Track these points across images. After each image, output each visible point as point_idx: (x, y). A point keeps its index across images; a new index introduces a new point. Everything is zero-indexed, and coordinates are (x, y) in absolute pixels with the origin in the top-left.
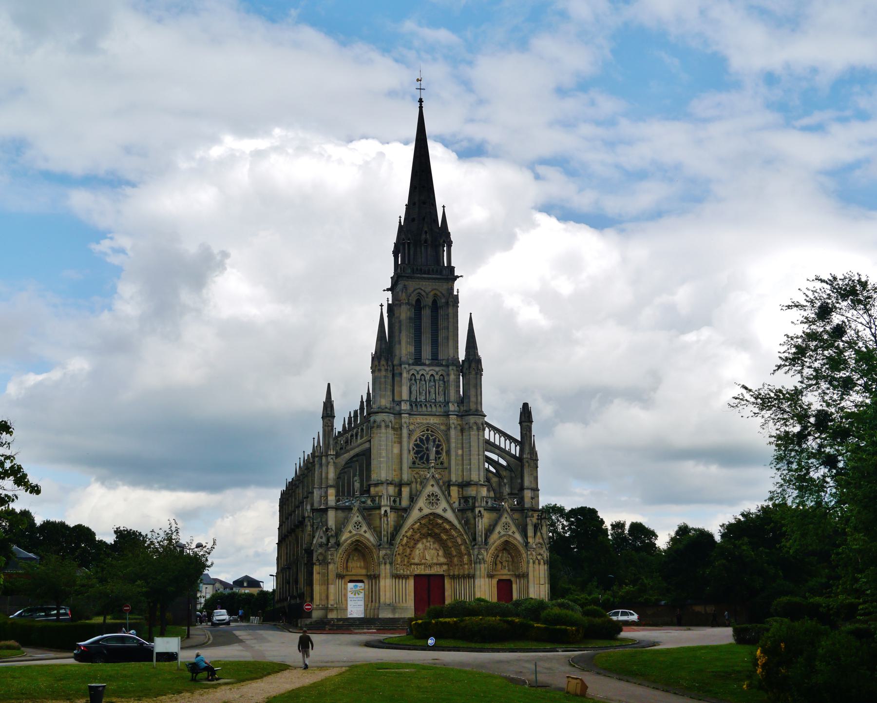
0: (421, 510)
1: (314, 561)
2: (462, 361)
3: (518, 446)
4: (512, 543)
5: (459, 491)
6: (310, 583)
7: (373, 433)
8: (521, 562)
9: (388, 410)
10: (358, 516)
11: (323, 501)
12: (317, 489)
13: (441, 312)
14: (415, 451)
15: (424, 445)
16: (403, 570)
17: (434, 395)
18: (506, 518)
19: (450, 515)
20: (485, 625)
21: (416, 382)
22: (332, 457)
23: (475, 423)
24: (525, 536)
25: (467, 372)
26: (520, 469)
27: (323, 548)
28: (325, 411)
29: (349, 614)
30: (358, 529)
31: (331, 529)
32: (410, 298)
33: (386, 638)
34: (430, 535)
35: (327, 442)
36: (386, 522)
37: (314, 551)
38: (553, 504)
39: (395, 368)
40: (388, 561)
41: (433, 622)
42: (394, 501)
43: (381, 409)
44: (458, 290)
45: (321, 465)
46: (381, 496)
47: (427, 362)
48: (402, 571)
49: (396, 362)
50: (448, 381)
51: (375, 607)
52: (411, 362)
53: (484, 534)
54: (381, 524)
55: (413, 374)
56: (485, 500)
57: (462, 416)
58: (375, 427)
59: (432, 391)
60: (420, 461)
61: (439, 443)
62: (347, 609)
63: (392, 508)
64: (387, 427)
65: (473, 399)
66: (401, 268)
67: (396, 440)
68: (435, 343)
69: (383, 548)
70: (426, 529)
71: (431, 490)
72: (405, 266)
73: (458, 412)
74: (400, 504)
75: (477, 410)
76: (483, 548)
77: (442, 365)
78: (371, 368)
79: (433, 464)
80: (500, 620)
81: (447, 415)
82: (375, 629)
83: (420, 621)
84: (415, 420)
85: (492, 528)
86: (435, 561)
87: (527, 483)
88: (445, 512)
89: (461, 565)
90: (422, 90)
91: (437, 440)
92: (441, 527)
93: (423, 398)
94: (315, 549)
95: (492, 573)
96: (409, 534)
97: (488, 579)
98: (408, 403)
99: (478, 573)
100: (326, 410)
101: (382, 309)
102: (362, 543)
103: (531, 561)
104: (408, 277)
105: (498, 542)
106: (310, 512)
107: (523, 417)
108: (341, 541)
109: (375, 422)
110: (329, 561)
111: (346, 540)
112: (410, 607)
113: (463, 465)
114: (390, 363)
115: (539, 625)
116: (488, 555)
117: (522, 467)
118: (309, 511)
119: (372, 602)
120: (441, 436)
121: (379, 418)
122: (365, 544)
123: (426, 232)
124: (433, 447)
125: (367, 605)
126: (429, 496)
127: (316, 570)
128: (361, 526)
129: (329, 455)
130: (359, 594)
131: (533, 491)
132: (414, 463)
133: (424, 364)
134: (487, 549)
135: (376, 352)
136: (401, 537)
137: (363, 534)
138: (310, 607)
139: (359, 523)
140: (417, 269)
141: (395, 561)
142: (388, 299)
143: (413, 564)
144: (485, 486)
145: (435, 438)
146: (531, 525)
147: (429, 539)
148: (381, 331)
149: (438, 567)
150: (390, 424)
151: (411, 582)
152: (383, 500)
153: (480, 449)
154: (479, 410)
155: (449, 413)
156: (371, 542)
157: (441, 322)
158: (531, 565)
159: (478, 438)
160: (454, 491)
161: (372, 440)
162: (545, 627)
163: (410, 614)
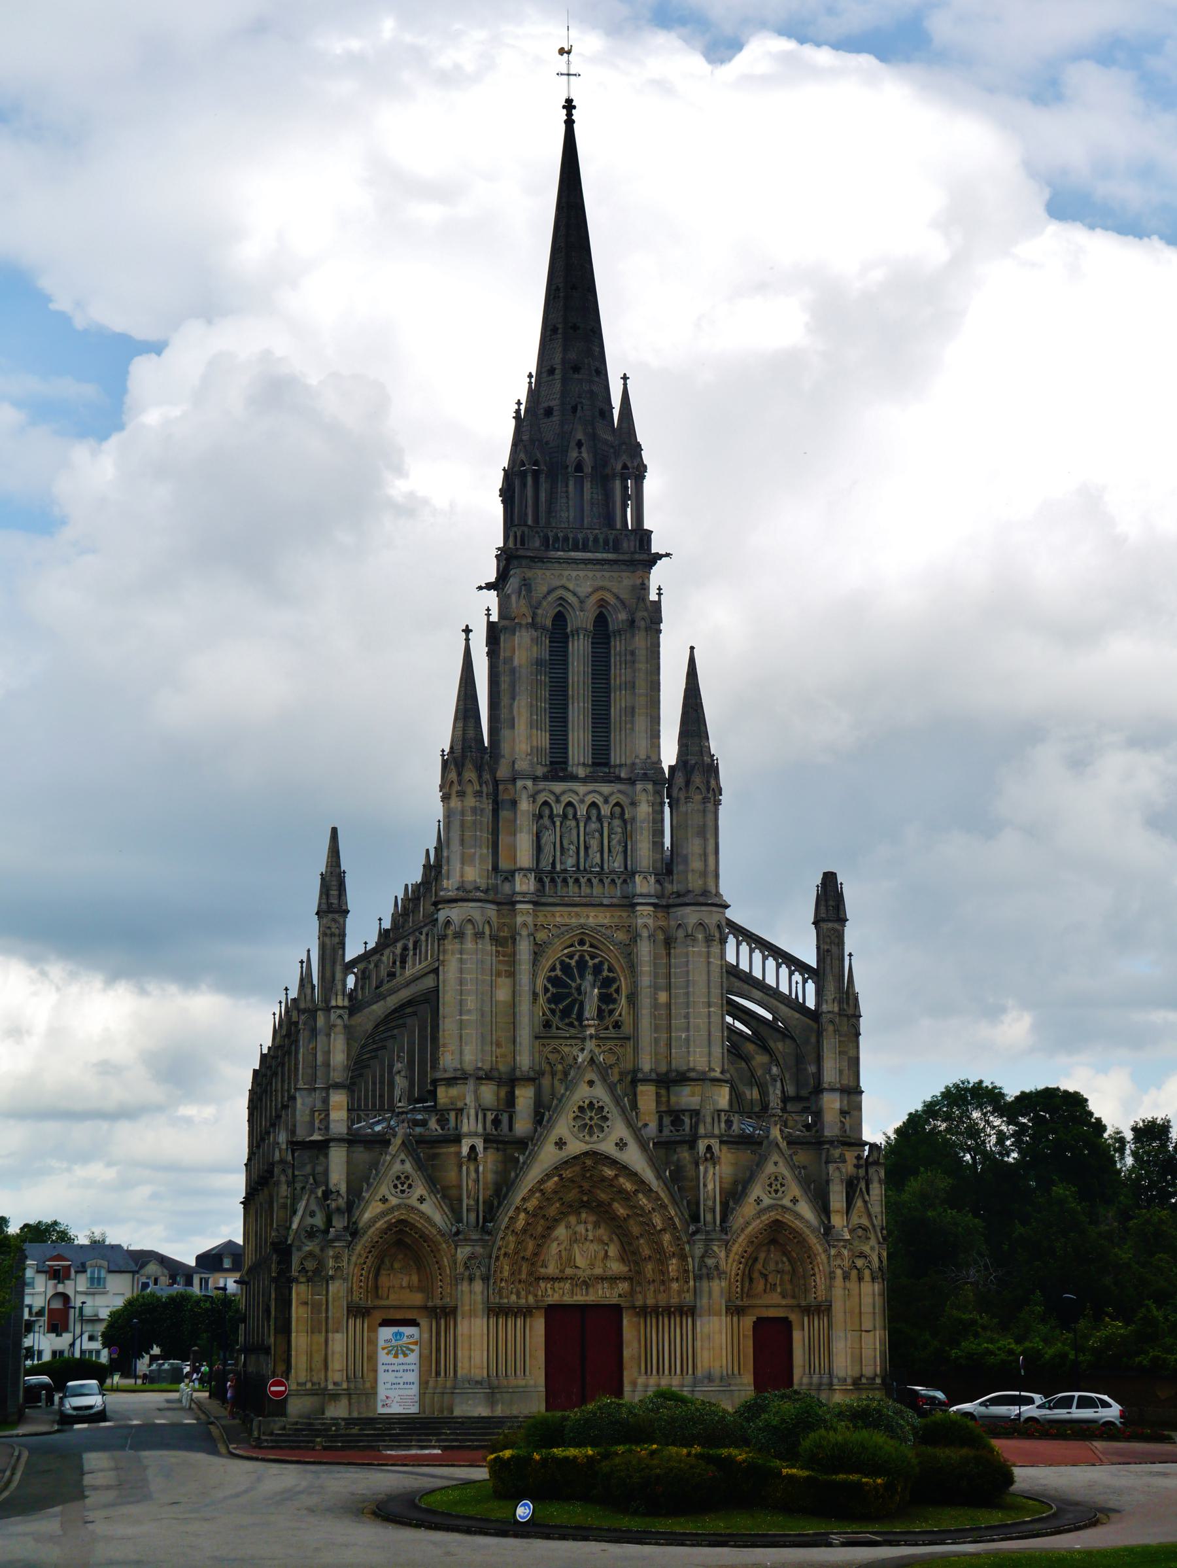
0: (560, 1144)
1: (294, 1274)
2: (671, 767)
3: (810, 981)
4: (790, 1227)
5: (657, 1093)
6: (285, 1329)
7: (444, 951)
8: (814, 1275)
9: (482, 894)
10: (403, 1162)
11: (317, 1122)
12: (305, 1093)
13: (617, 645)
14: (549, 995)
15: (574, 980)
16: (518, 1297)
17: (598, 855)
18: (776, 1163)
19: (634, 1157)
20: (658, 1471)
21: (554, 823)
22: (339, 1012)
23: (700, 923)
24: (824, 1209)
25: (682, 796)
26: (813, 1040)
27: (317, 1241)
28: (324, 897)
29: (380, 1404)
30: (403, 1192)
31: (338, 1191)
32: (540, 611)
33: (440, 1483)
34: (585, 1205)
35: (328, 974)
36: (473, 1175)
37: (294, 1249)
38: (973, 1080)
39: (501, 787)
40: (478, 1274)
41: (537, 1457)
42: (496, 1122)
43: (465, 890)
44: (659, 589)
45: (314, 1032)
46: (461, 1110)
47: (581, 772)
48: (514, 1297)
49: (503, 772)
50: (633, 819)
51: (445, 1388)
52: (540, 771)
53: (721, 1202)
54: (461, 1180)
55: (546, 803)
56: (723, 1118)
57: (668, 906)
58: (450, 937)
59: (594, 844)
60: (562, 1019)
61: (611, 975)
62: (375, 1394)
63: (487, 1140)
64: (479, 935)
65: (696, 864)
66: (516, 537)
67: (503, 968)
68: (601, 722)
69: (466, 1240)
70: (577, 1190)
71: (586, 1095)
72: (526, 529)
73: (657, 897)
74: (511, 1128)
75: (705, 893)
76: (719, 1240)
77: (619, 779)
78: (442, 787)
79: (592, 1031)
80: (699, 1456)
81: (629, 904)
82: (439, 1447)
83: (507, 1453)
84: (550, 919)
85: (740, 1188)
86: (598, 1271)
87: (830, 1075)
88: (621, 1149)
89: (663, 1282)
90: (572, 78)
91: (606, 967)
92: (611, 1186)
93: (570, 861)
94: (297, 1243)
95: (739, 1303)
96: (531, 1205)
97: (729, 1319)
99: (704, 1301)
100: (328, 896)
101: (467, 640)
102: (413, 1226)
103: (839, 1272)
104: (532, 559)
105: (755, 1225)
106: (287, 1149)
107: (823, 909)
108: (361, 1225)
109: (448, 923)
110: (331, 1273)
111: (373, 1221)
112: (535, 1386)
113: (669, 1029)
114: (487, 776)
115: (794, 1471)
116: (728, 1259)
117: (819, 1034)
118: (284, 1146)
119: (438, 1374)
120: (613, 956)
121: (455, 914)
123: (579, 444)
124: (593, 986)
125: (427, 1382)
126: (581, 1109)
127: (298, 1294)
128: (410, 1186)
129: (333, 1007)
130: (405, 1355)
131: (845, 1098)
132: (547, 1025)
133: (574, 778)
134: (727, 1242)
135: (452, 748)
136: (510, 1213)
137: (416, 1204)
138: (283, 1388)
139: (407, 1178)
140: (556, 538)
141: (495, 1271)
142: (488, 610)
143: (543, 1278)
144: (726, 1081)
145: (601, 963)
146: (837, 1180)
147: (584, 1215)
148: (466, 694)
149: (606, 1285)
150: (487, 932)
151: (539, 1325)
152: (465, 1121)
153: (712, 990)
154: (709, 892)
155: (635, 901)
156: (434, 1225)
157: (618, 671)
158: (839, 1282)
159: (709, 963)
160: (647, 1097)
161: (441, 968)
162: (808, 1477)
163: (536, 1406)
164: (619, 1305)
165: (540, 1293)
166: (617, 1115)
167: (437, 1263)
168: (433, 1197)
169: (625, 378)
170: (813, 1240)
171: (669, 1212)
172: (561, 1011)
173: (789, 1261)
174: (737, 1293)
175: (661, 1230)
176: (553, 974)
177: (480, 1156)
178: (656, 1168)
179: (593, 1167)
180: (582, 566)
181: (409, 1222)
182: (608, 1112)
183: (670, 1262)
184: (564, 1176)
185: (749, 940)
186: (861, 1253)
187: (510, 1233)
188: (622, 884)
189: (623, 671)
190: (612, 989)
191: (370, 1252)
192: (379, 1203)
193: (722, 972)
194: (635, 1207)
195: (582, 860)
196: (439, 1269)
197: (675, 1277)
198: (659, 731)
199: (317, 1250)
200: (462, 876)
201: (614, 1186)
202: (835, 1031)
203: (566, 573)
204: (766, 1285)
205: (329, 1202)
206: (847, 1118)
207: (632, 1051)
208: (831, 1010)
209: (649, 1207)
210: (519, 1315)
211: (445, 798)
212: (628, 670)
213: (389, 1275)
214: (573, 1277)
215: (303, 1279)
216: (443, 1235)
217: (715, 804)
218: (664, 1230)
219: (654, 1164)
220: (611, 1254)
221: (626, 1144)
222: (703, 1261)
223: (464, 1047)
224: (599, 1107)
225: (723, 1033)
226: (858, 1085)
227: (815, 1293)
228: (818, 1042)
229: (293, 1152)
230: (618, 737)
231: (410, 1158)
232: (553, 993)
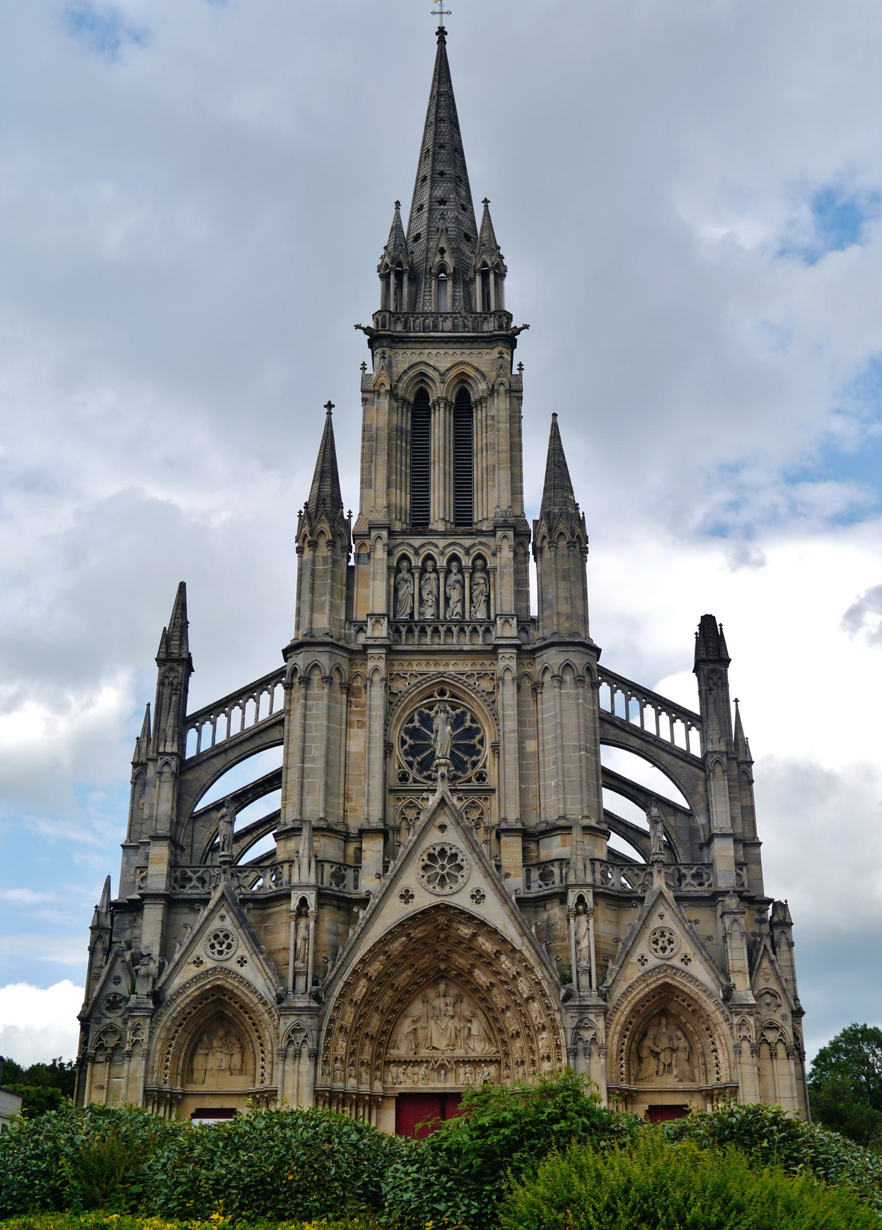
0: (407, 896)
2: (535, 522)
4: (683, 991)
5: (525, 849)
8: (715, 1051)
10: (222, 918)
13: (479, 415)
16: (359, 1082)
17: (459, 605)
18: (661, 916)
21: (413, 575)
22: (166, 758)
24: (722, 970)
26: (701, 789)
28: (164, 646)
30: (220, 952)
34: (442, 975)
38: (861, 1024)
44: (520, 365)
55: (404, 557)
59: (455, 595)
61: (474, 725)
63: (323, 897)
71: (437, 842)
74: (356, 887)
77: (481, 533)
79: (442, 770)
86: (459, 1053)
88: (478, 902)
91: (468, 717)
92: (471, 949)
93: (429, 614)
95: (624, 1085)
96: (374, 969)
98: (385, 622)
100: (168, 647)
101: (329, 413)
102: (232, 995)
103: (745, 1045)
108: (170, 991)
111: (184, 987)
122: (239, 997)
123: (442, 251)
126: (431, 856)
128: (229, 946)
132: (404, 778)
133: (435, 533)
137: (236, 967)
139: (226, 936)
145: (464, 714)
146: (736, 935)
147: (442, 987)
148: (324, 458)
150: (337, 679)
156: (255, 992)
166: (473, 863)
167: (259, 1038)
168: (255, 958)
169: (486, 201)
170: (710, 1006)
171: (536, 975)
172: (418, 763)
173: (685, 1036)
174: (622, 1074)
175: (528, 999)
176: (410, 725)
178: (519, 924)
179: (447, 925)
180: (443, 345)
181: (227, 989)
182: (462, 860)
183: (540, 1037)
184: (412, 935)
185: (624, 687)
186: (771, 1023)
187: (347, 1003)
188: (484, 632)
189: (484, 434)
190: (476, 740)
191: (181, 1025)
192: (193, 966)
193: (594, 718)
194: (498, 973)
195: (442, 610)
196: (261, 1045)
197: (545, 1055)
198: (522, 488)
199: (119, 1023)
200: (311, 623)
201: (474, 949)
202: (724, 772)
203: (427, 351)
204: (658, 1066)
205: (137, 967)
206: (745, 869)
207: (497, 803)
208: (717, 749)
209: (513, 971)
210: (361, 1104)
211: (300, 551)
212: (489, 433)
213: (207, 1055)
214: (429, 1059)
215: (101, 1059)
216: (265, 1004)
217: (581, 552)
218: (531, 998)
219: (516, 918)
221: (483, 896)
222: (578, 1033)
223: (305, 797)
224: (452, 854)
225: (598, 781)
226: (755, 836)
227: (718, 1073)
228: (706, 791)
229: (112, 917)
230: (480, 496)
231: (231, 913)
232: (410, 746)
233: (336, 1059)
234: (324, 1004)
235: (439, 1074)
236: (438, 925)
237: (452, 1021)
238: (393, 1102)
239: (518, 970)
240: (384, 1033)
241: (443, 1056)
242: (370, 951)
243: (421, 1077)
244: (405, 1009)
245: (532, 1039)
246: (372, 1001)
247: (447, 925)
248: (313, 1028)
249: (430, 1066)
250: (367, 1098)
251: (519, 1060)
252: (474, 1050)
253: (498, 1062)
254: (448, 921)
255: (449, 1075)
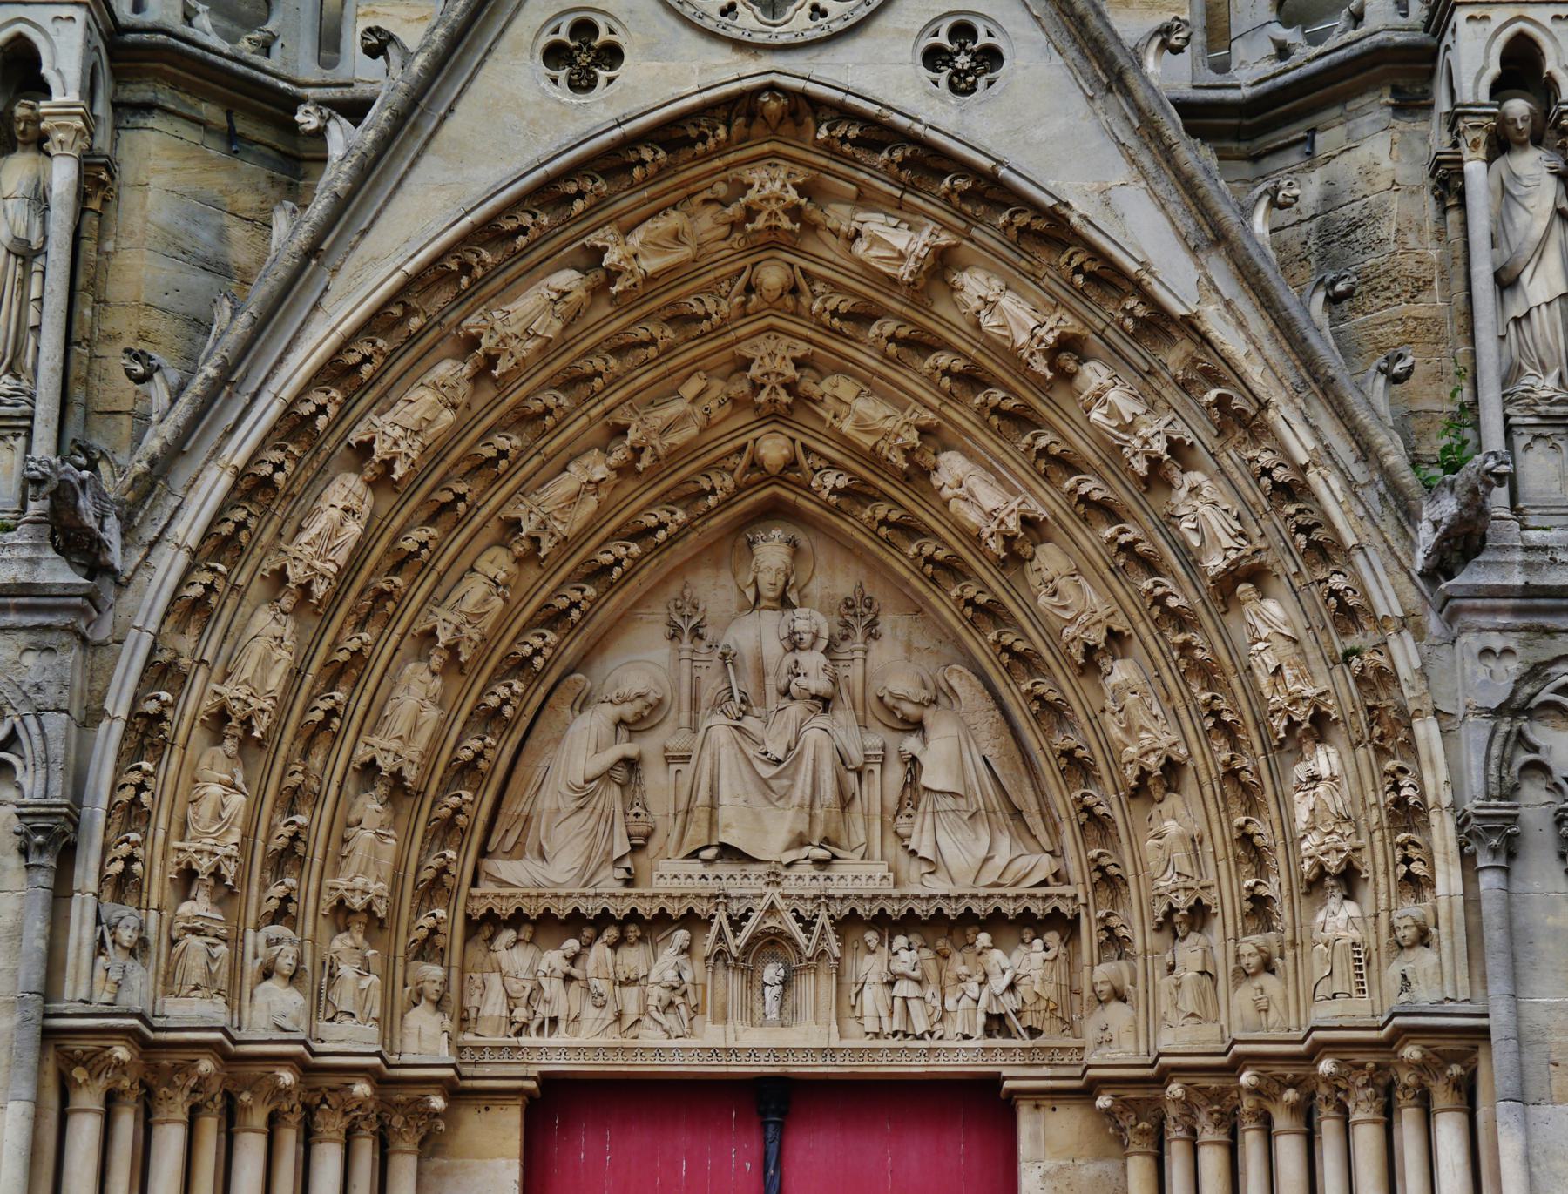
16: (321, 1004)
88: (961, 86)
92: (922, 344)
147: (771, 553)
164: (995, 1080)
165: (494, 1006)
171: (1283, 450)
175: (1226, 588)
177: (57, 98)
179: (795, 212)
183: (1300, 771)
194: (1067, 464)
197: (1333, 862)
209: (1153, 434)
210: (331, 1124)
214: (702, 908)
220: (932, 776)
221: (992, 57)
222: (1521, 739)
233: (188, 876)
234: (122, 585)
235: (751, 978)
236: (750, 213)
237: (822, 720)
238: (507, 1125)
239: (1180, 431)
240: (466, 772)
241: (773, 893)
242: (377, 322)
243: (656, 993)
244: (583, 662)
245: (1250, 796)
246: (401, 601)
247: (795, 212)
248: (50, 696)
249: (708, 943)
250: (362, 1089)
251: (1182, 902)
252: (933, 866)
253: (1066, 926)
254: (802, 190)
255: (806, 986)
